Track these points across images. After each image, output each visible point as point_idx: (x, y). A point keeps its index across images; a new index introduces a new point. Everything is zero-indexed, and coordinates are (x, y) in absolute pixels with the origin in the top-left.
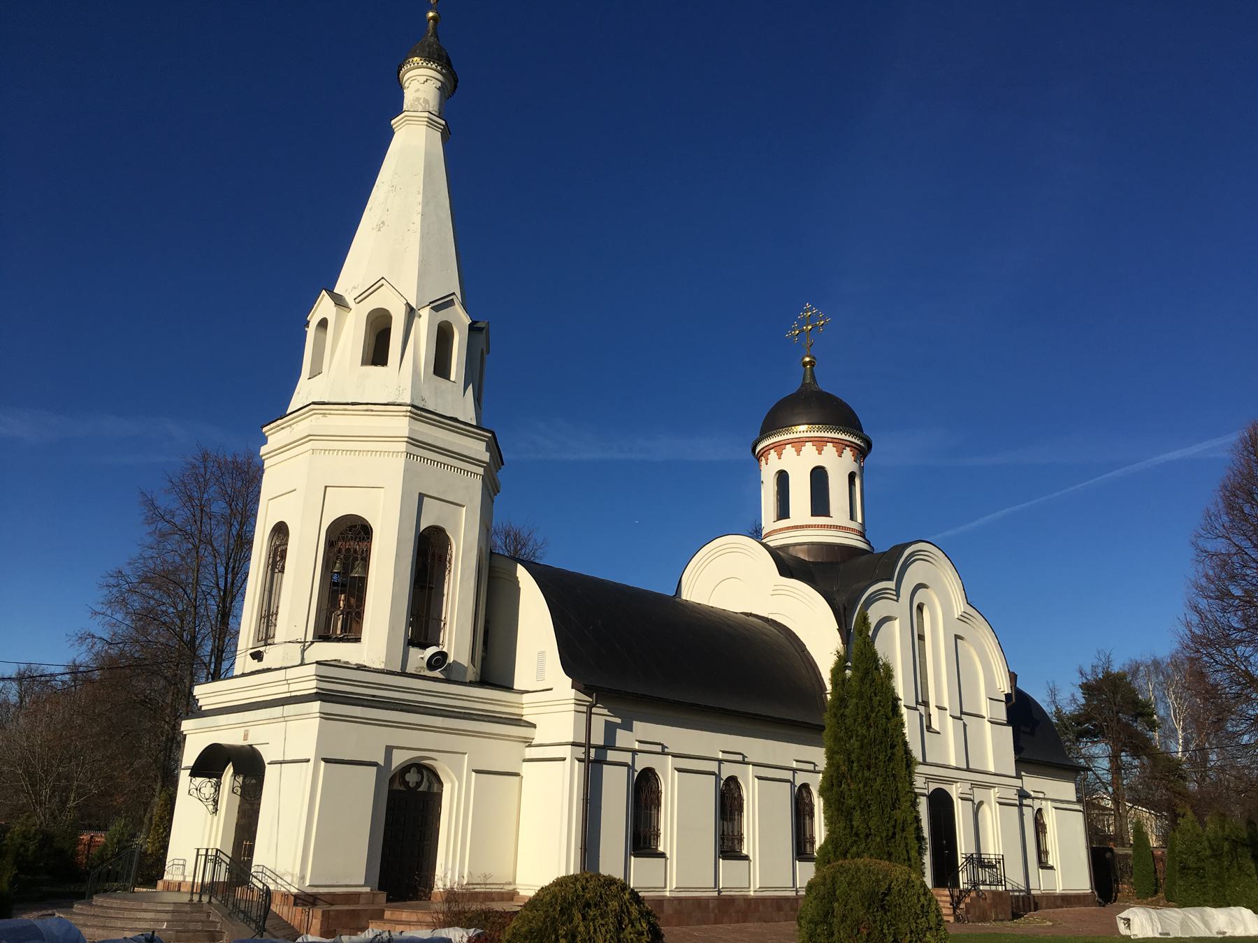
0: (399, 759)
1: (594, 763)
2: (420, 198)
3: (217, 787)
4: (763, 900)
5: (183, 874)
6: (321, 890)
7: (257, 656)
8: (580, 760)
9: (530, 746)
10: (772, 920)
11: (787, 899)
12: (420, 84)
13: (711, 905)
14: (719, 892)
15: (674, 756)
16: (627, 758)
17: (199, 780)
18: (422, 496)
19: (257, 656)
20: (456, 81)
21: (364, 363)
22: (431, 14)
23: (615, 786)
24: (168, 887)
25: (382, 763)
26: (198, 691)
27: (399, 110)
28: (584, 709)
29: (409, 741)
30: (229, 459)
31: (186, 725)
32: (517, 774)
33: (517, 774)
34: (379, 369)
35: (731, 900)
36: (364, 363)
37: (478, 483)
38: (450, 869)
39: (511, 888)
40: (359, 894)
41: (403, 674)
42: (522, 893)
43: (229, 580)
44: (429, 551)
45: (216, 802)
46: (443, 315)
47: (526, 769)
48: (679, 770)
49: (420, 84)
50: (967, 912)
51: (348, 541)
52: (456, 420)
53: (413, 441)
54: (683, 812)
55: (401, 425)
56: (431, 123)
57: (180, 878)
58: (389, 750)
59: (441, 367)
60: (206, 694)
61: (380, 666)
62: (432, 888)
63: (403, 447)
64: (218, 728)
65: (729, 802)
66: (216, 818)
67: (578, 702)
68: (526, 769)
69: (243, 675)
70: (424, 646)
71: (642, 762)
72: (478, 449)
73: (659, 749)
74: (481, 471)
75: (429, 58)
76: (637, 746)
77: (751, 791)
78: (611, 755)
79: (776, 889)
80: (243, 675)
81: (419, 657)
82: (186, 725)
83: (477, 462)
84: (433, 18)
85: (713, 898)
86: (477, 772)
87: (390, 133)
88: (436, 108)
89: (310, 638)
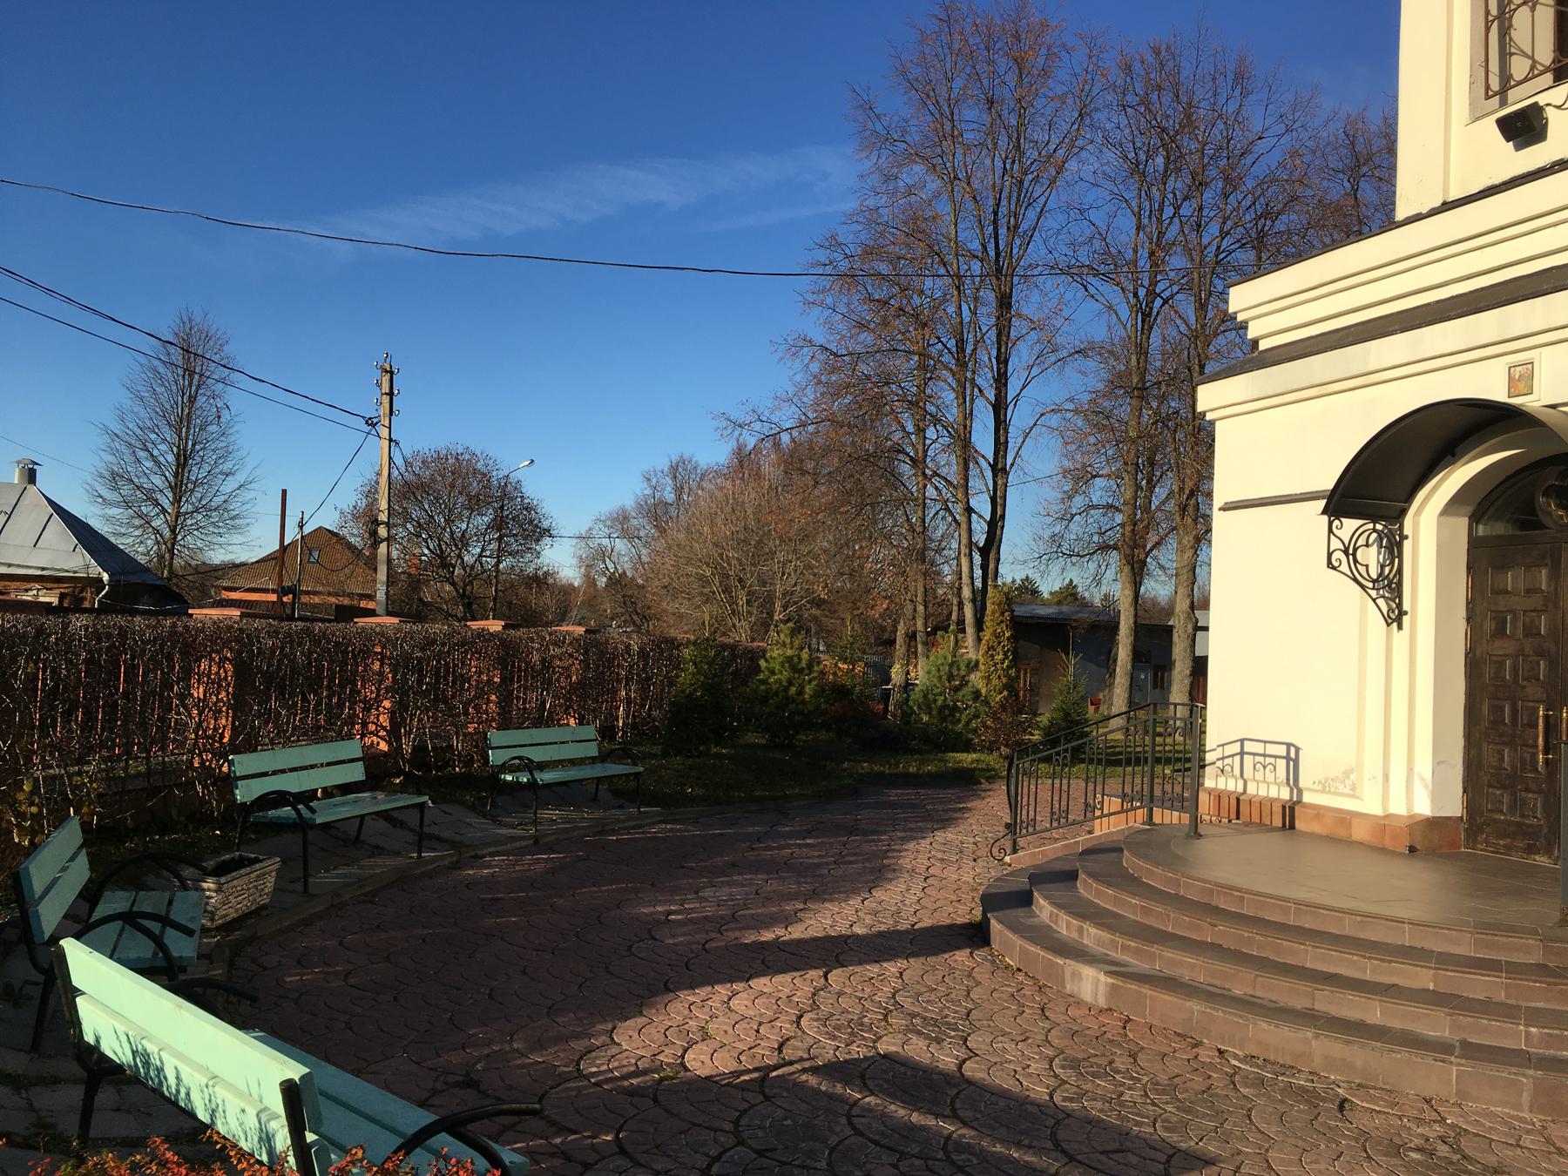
3: (1393, 546)
5: (1293, 779)
7: (1524, 127)
17: (1349, 525)
19: (1524, 127)
24: (1236, 807)
26: (1241, 298)
31: (1210, 397)
45: (1390, 586)
57: (1285, 794)
60: (1264, 303)
64: (1367, 379)
66: (1400, 638)
69: (1447, 206)
80: (1447, 206)
82: (1210, 397)
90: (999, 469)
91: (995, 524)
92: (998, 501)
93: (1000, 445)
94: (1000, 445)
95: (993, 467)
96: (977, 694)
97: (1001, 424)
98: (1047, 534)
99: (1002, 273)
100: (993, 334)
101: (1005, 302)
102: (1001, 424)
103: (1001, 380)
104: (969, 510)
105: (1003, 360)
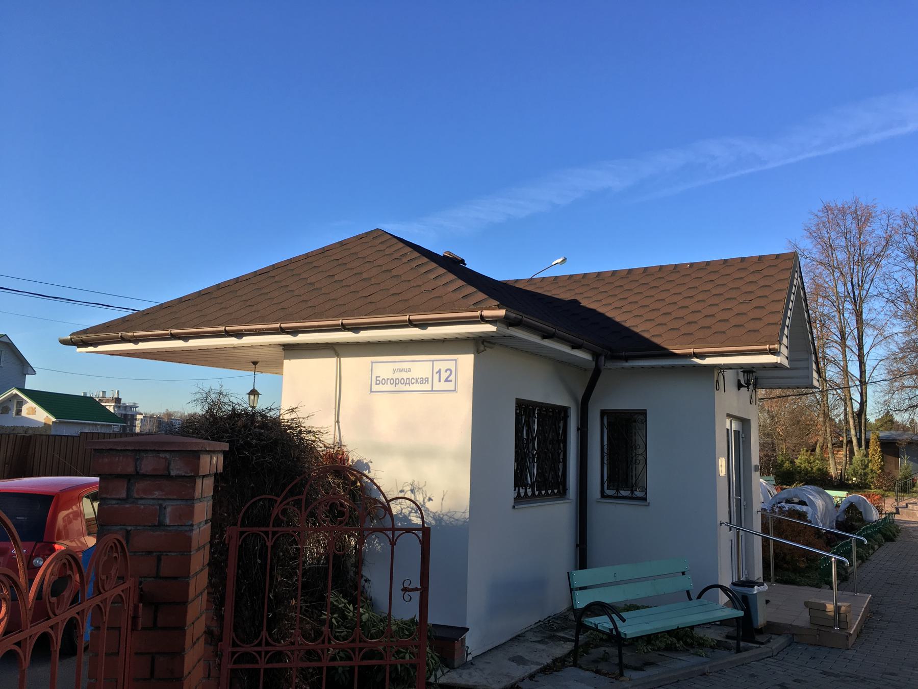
30: (840, 205)
43: (857, 293)
90: (863, 383)
91: (863, 404)
92: (863, 395)
93: (862, 372)
94: (862, 372)
95: (860, 381)
96: (872, 471)
97: (862, 364)
98: (882, 400)
99: (858, 304)
100: (856, 332)
101: (859, 314)
102: (862, 364)
103: (861, 347)
104: (851, 399)
105: (860, 338)
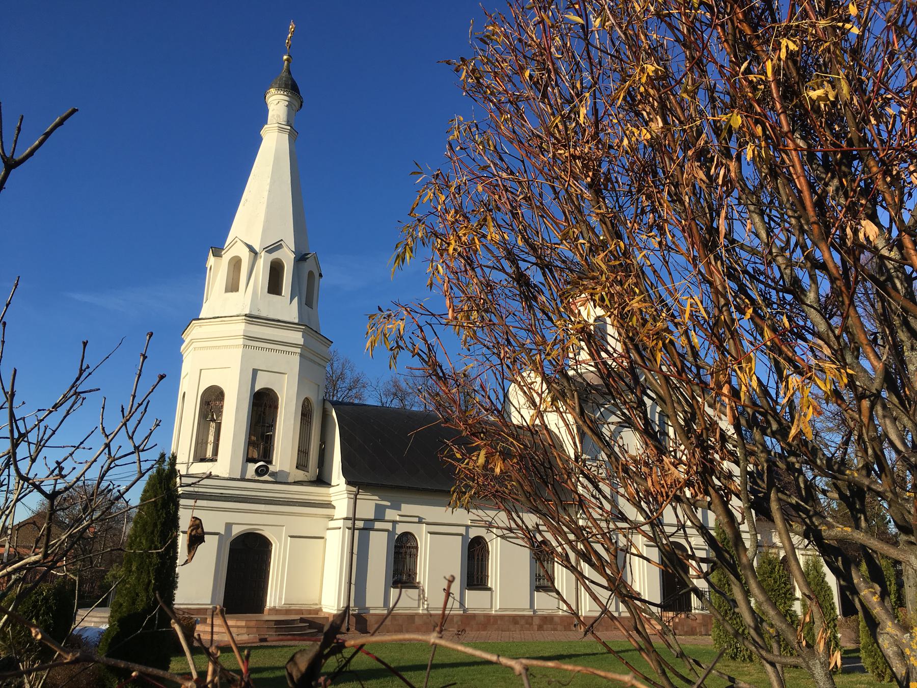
0: (236, 531)
1: (360, 531)
2: (269, 180)
4: (502, 617)
6: (182, 607)
8: (349, 528)
9: (332, 520)
10: (509, 630)
11: (523, 617)
12: (277, 103)
13: (455, 620)
14: (465, 610)
15: (428, 524)
16: (389, 526)
18: (255, 372)
20: (301, 98)
21: (226, 291)
22: (285, 57)
23: (379, 546)
25: (223, 533)
27: (265, 121)
28: (352, 496)
29: (245, 520)
32: (322, 538)
33: (322, 538)
34: (234, 293)
35: (474, 616)
36: (226, 291)
37: (297, 358)
38: (277, 595)
39: (318, 607)
40: (207, 609)
41: (243, 479)
42: (324, 610)
44: (263, 405)
46: (275, 255)
47: (329, 535)
48: (431, 533)
49: (277, 103)
50: (675, 628)
51: (212, 401)
52: (279, 321)
53: (248, 338)
54: (437, 560)
55: (240, 327)
56: (281, 130)
58: (229, 526)
59: (274, 287)
61: (227, 476)
62: (264, 606)
63: (241, 341)
65: (476, 553)
67: (349, 492)
68: (329, 535)
70: (255, 461)
71: (400, 529)
72: (297, 337)
73: (416, 520)
74: (299, 350)
75: (279, 88)
76: (398, 518)
77: (496, 547)
78: (378, 525)
79: (515, 610)
81: (252, 467)
83: (295, 345)
84: (288, 60)
85: (460, 615)
86: (291, 537)
87: (260, 139)
88: (285, 119)
89: (191, 460)
